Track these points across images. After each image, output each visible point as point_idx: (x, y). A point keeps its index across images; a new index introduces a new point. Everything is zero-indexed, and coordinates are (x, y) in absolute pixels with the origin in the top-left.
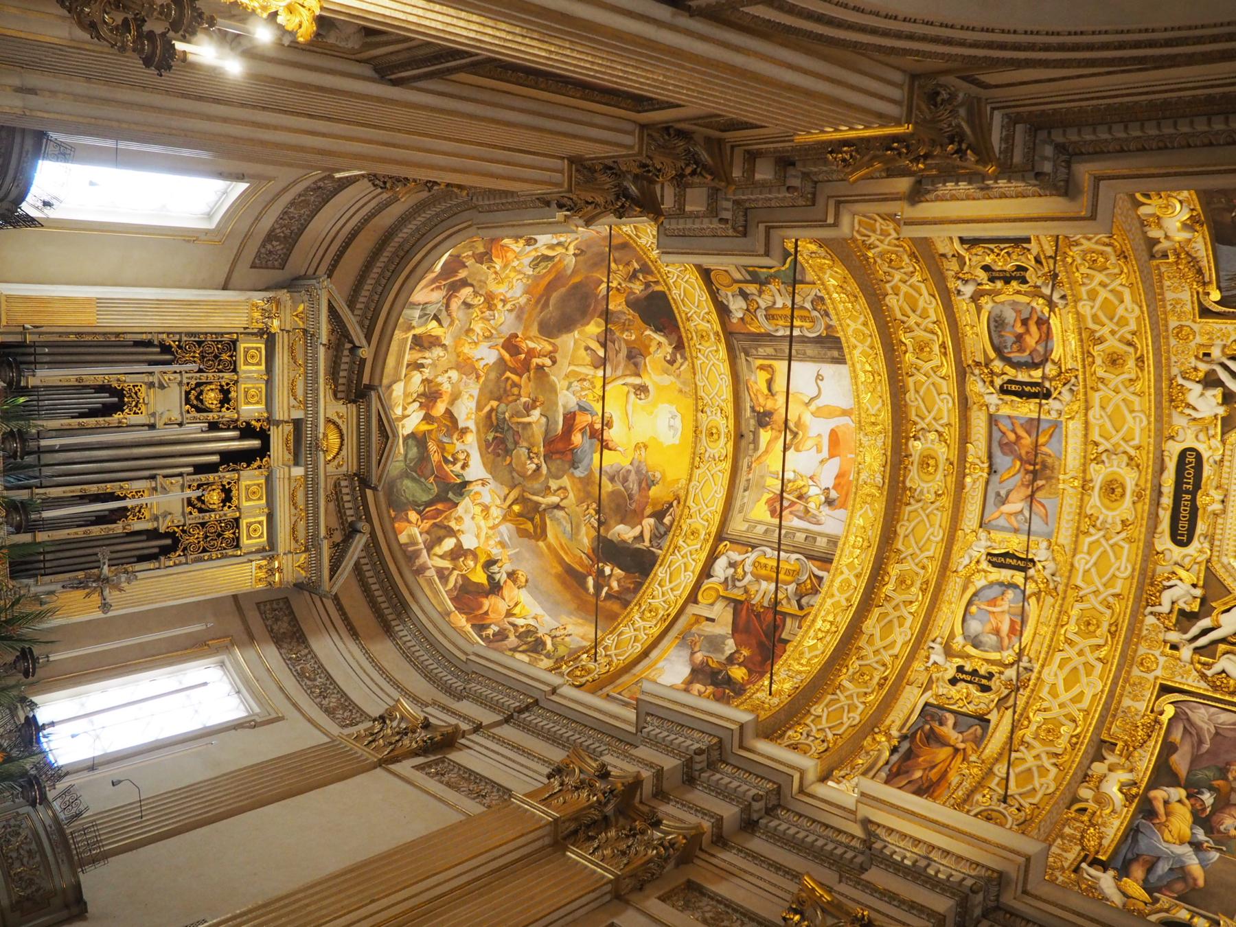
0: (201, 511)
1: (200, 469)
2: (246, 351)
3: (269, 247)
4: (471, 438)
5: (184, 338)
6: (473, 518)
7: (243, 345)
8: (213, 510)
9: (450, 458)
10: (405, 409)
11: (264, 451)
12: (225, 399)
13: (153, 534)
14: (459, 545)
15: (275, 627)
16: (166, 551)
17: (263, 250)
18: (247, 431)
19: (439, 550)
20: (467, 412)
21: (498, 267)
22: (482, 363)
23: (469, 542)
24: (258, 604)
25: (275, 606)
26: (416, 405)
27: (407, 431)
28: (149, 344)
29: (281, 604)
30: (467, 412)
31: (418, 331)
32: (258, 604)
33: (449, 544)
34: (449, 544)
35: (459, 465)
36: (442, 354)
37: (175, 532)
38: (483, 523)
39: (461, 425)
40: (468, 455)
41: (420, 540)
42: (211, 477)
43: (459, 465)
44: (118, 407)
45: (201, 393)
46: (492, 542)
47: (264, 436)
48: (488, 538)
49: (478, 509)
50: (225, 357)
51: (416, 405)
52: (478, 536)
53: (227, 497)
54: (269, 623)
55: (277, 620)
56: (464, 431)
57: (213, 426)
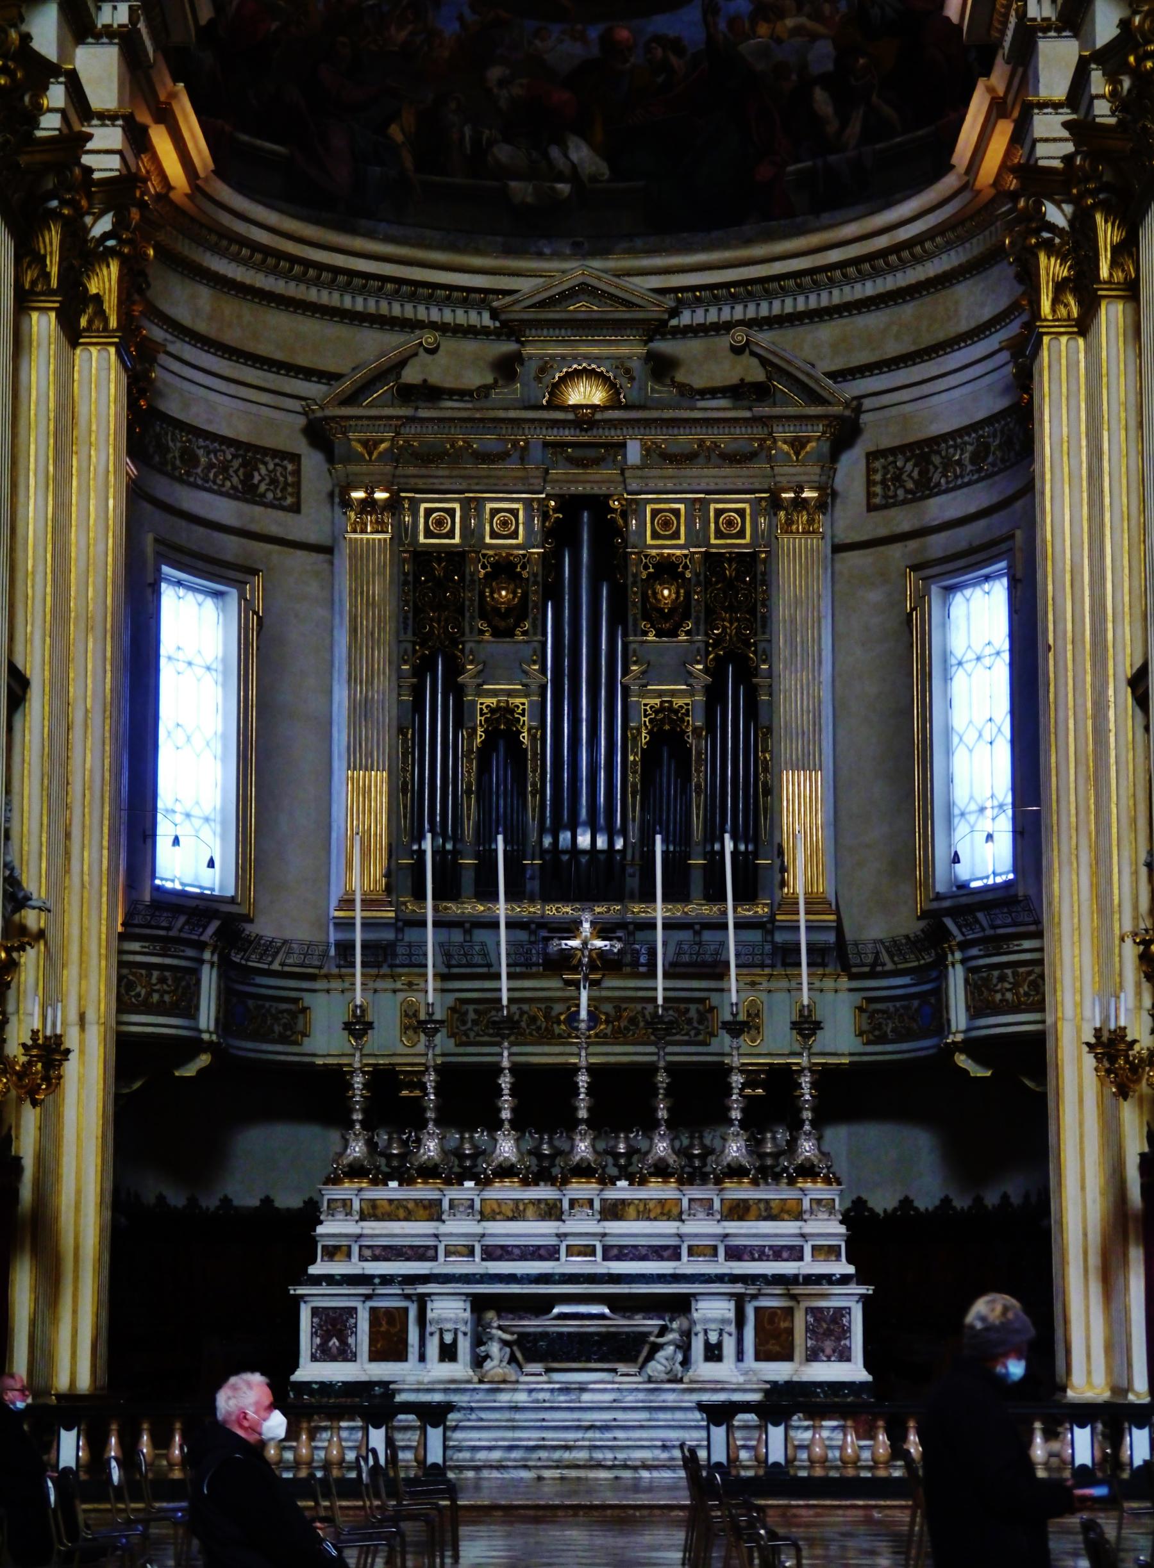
0: (686, 616)
1: (618, 618)
2: (429, 534)
3: (263, 488)
4: (623, 34)
5: (409, 636)
6: (779, 41)
7: (422, 540)
8: (688, 595)
9: (660, 80)
10: (561, 178)
11: (598, 504)
12: (505, 569)
13: (714, 695)
14: (825, 80)
15: (910, 485)
16: (747, 674)
17: (270, 495)
18: (560, 534)
19: (832, 127)
20: (564, 48)
21: (274, 26)
22: (469, 17)
23: (822, 55)
24: (871, 508)
25: (878, 477)
26: (555, 152)
27: (604, 169)
28: (418, 693)
29: (877, 464)
30: (564, 48)
31: (409, 163)
32: (871, 508)
33: (821, 98)
34: (821, 98)
35: (674, 59)
36: (453, 105)
37: (717, 657)
38: (790, 22)
39: (595, 52)
40: (658, 39)
41: (809, 163)
42: (634, 595)
43: (674, 59)
44: (513, 737)
45: (496, 610)
46: (827, 9)
47: (571, 505)
48: (816, 16)
49: (763, 29)
50: (439, 572)
51: (555, 152)
52: (814, 37)
53: (667, 569)
54: (900, 492)
55: (897, 478)
56: (606, 39)
57: (552, 592)
